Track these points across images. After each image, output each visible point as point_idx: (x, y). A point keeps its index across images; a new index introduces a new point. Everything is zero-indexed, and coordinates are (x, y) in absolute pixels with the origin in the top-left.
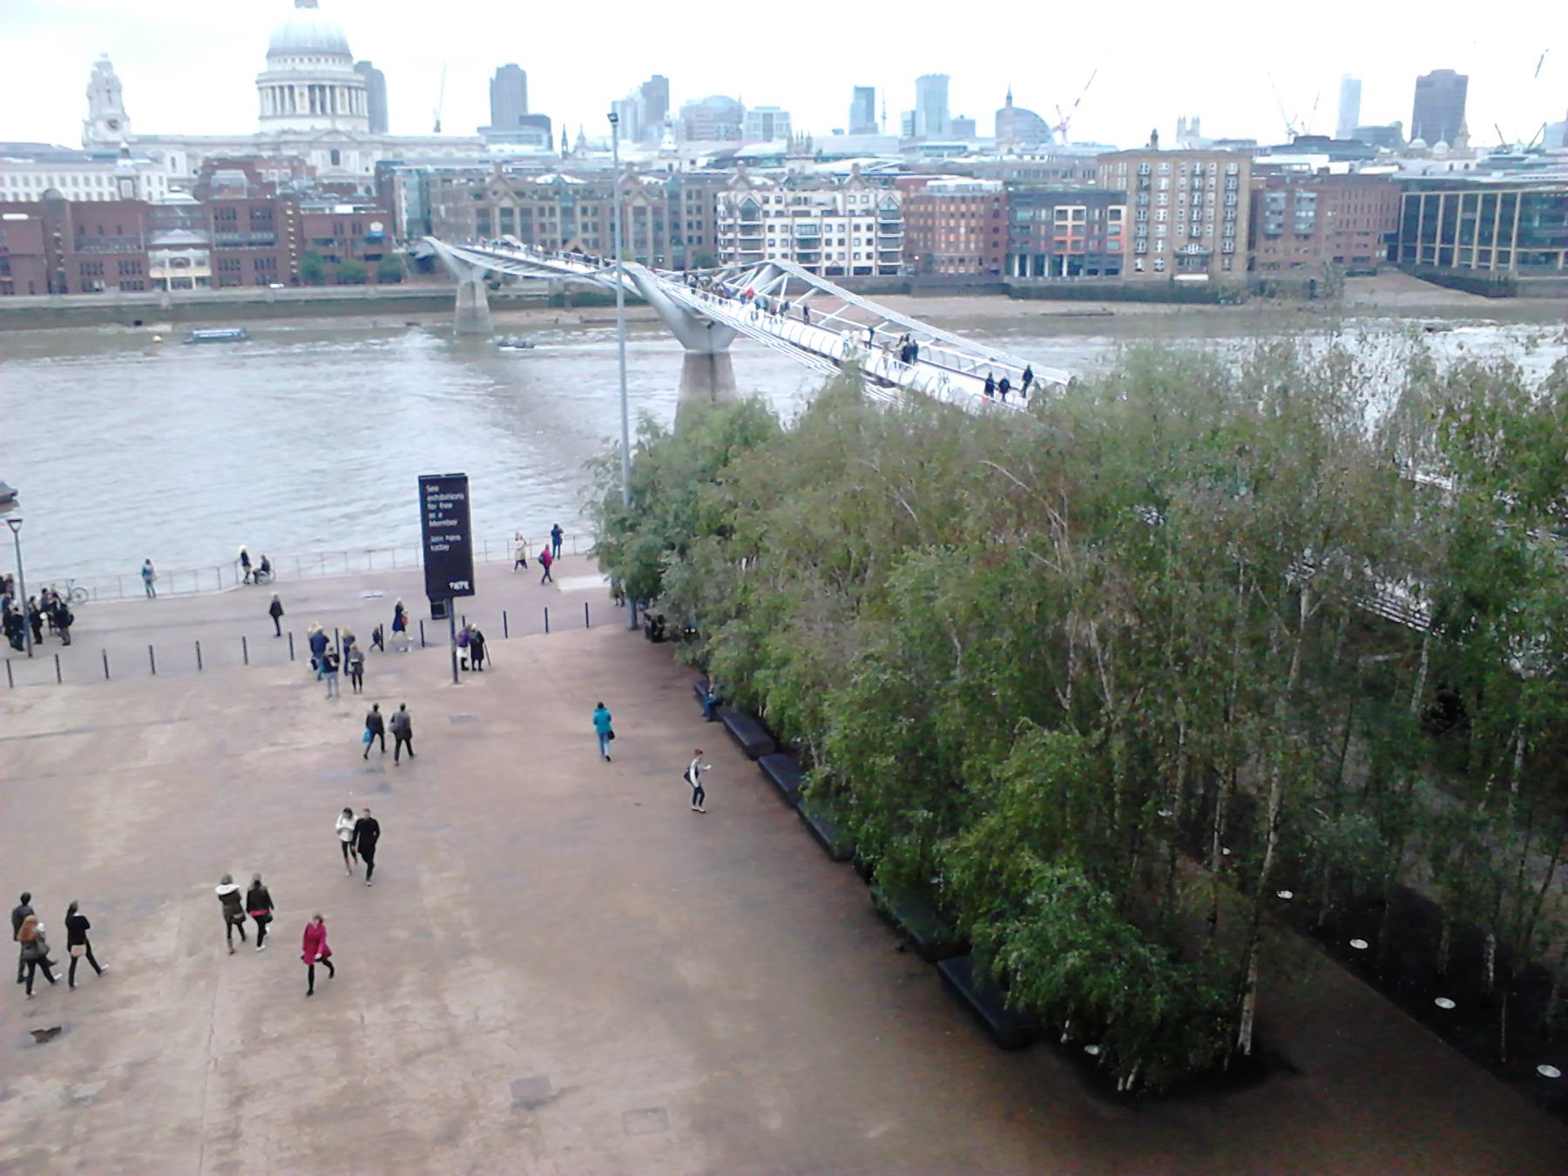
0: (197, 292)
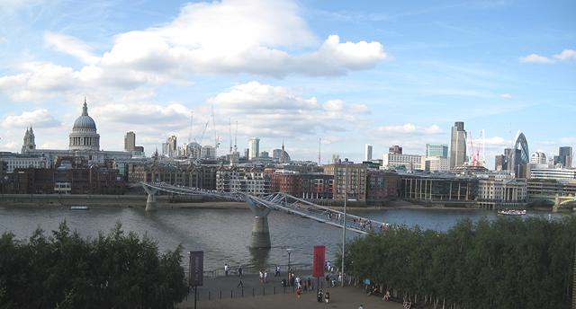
0: (67, 195)
